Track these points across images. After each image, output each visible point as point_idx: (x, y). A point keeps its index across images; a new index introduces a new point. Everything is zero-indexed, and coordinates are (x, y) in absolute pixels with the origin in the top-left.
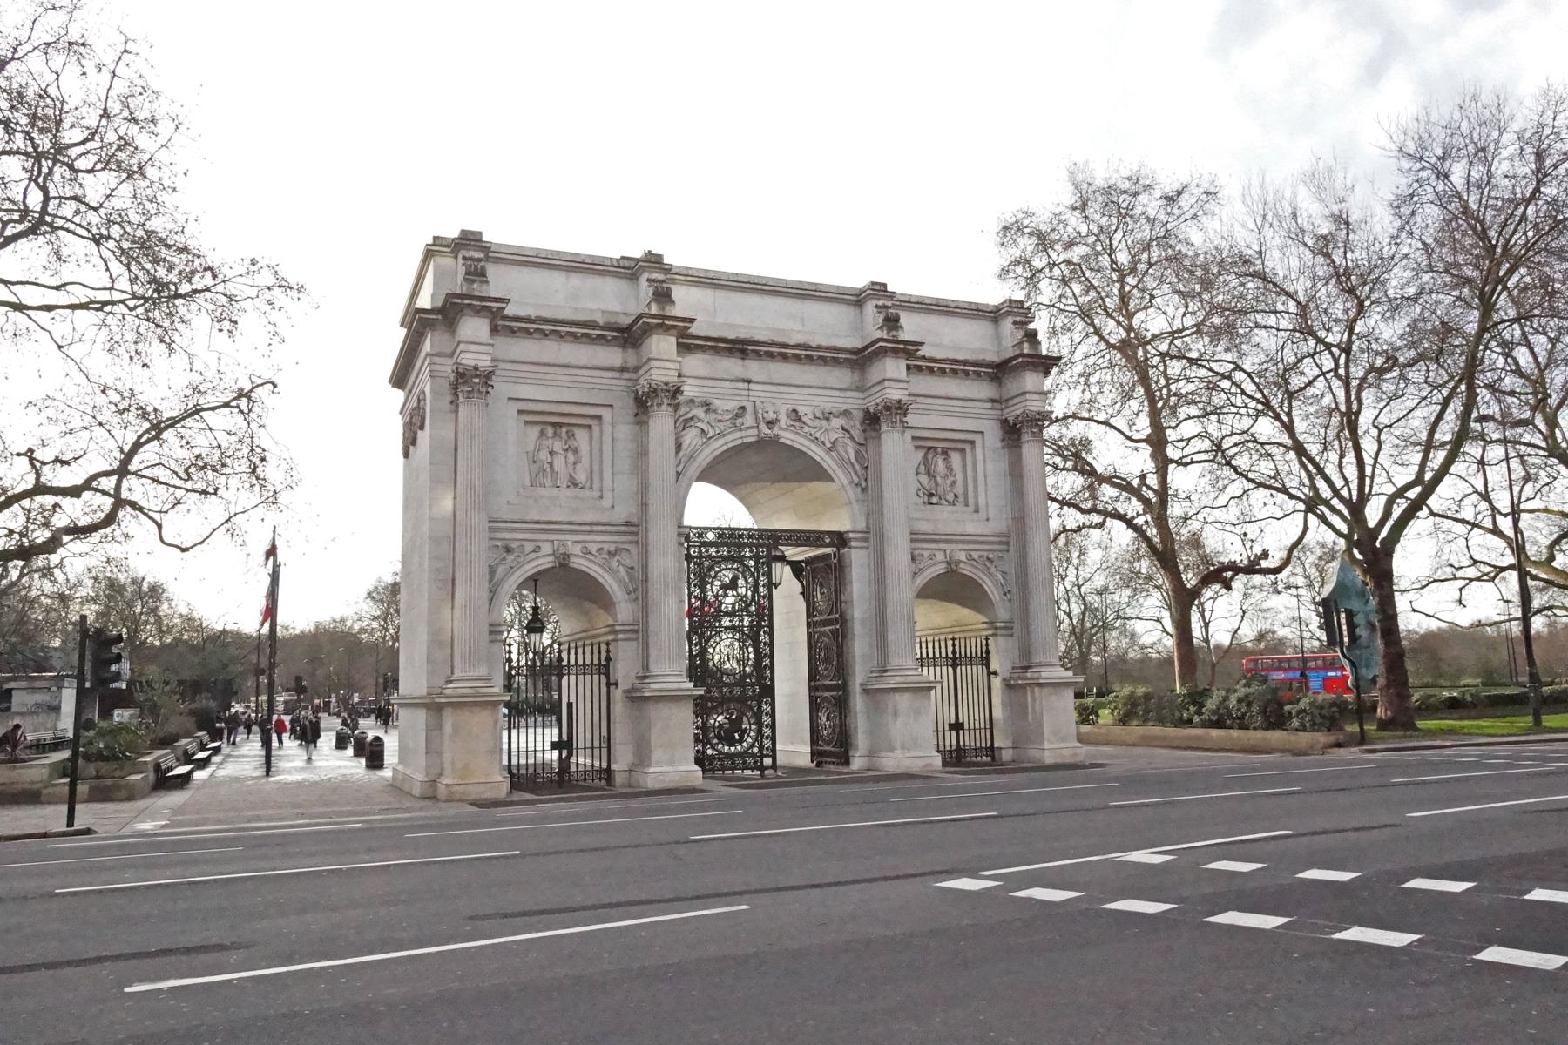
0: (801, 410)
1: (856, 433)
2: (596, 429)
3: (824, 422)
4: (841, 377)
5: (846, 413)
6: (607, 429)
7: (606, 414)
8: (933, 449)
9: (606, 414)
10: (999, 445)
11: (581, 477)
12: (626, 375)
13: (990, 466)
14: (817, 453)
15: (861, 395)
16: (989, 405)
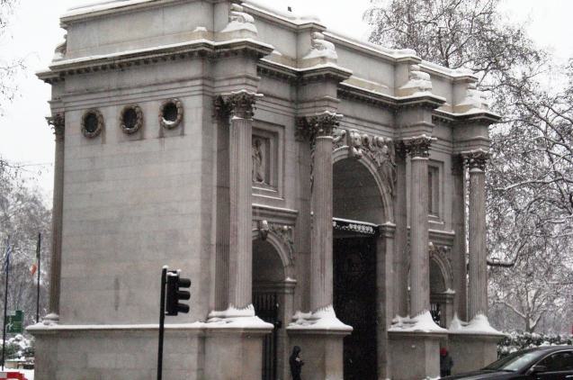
0: (370, 139)
1: (392, 158)
2: (272, 142)
3: (377, 148)
4: (382, 117)
5: (388, 144)
6: (281, 142)
7: (280, 131)
8: (433, 169)
9: (280, 131)
10: (450, 172)
11: (263, 175)
12: (293, 105)
13: (446, 185)
14: (373, 169)
15: (393, 131)
16: (447, 144)
